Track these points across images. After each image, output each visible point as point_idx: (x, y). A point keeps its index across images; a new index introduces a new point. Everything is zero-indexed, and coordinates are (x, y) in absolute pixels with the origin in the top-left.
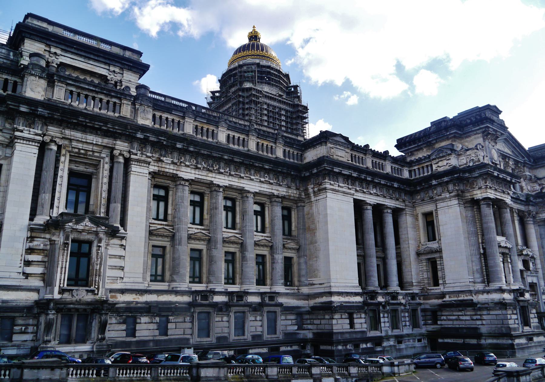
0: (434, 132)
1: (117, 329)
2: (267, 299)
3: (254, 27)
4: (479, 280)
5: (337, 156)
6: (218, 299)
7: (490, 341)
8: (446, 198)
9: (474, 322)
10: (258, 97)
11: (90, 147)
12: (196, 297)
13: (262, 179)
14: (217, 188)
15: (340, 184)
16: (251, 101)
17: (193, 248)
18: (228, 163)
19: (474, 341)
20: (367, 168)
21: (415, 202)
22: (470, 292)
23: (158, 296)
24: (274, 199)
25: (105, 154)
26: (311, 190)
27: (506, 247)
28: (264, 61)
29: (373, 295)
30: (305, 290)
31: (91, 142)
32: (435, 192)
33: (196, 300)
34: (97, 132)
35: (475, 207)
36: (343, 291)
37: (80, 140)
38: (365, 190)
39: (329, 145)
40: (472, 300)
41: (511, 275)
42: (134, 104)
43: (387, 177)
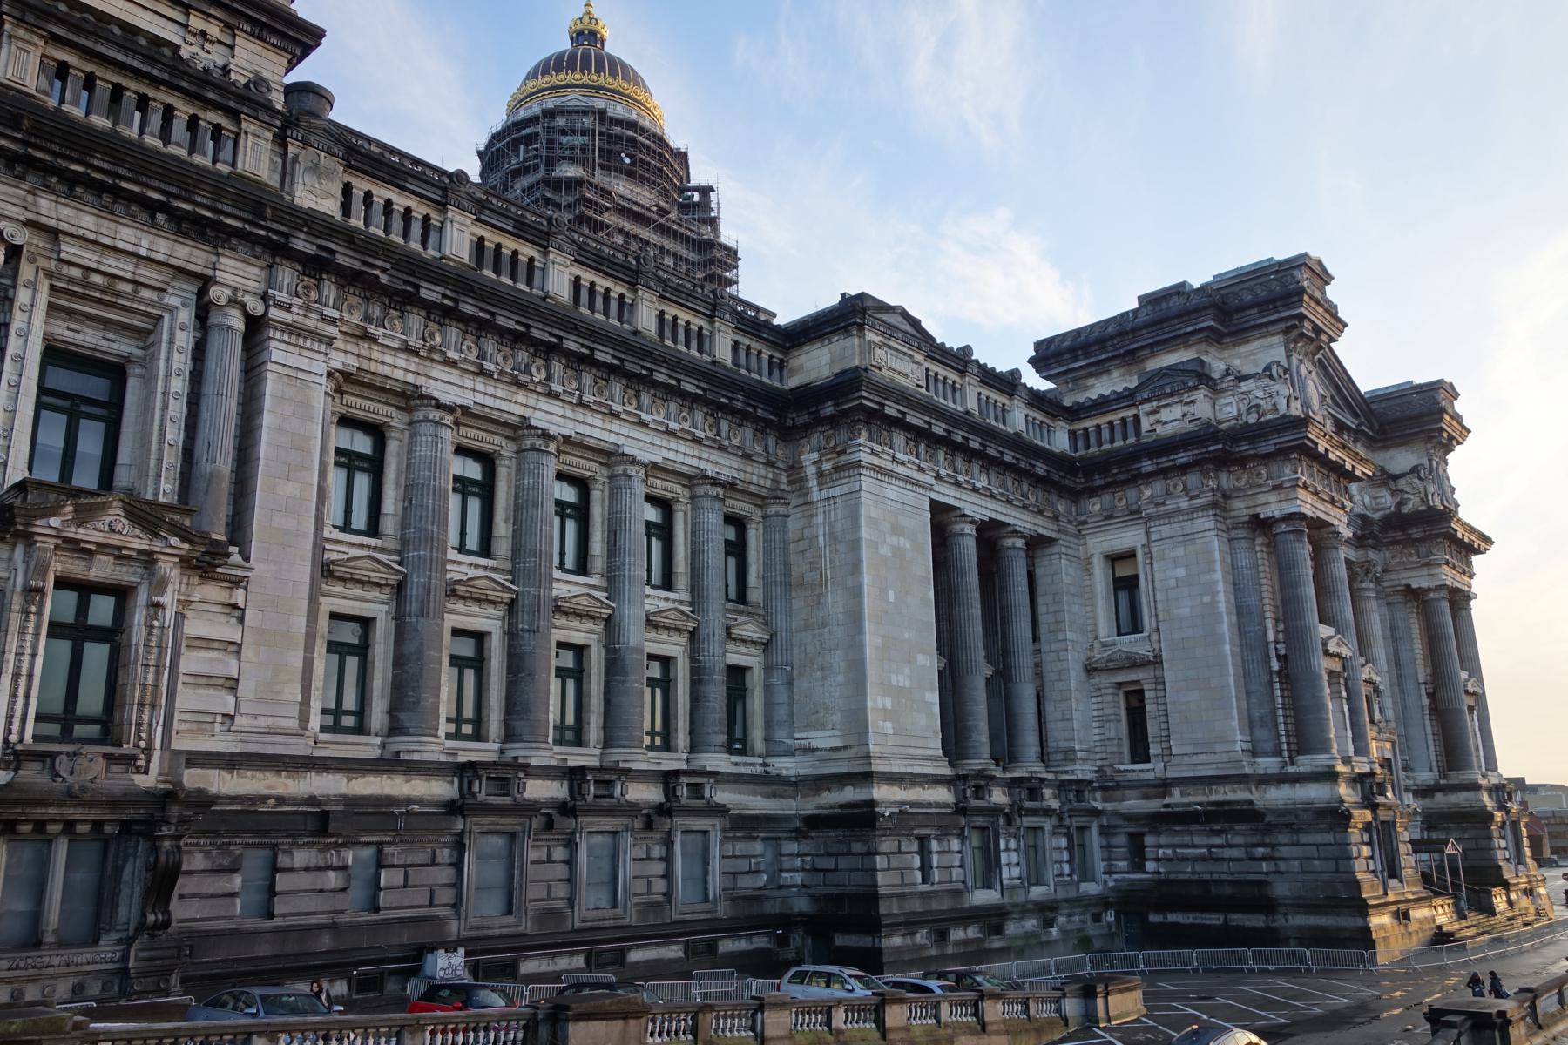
0: (1148, 325)
1: (211, 891)
2: (683, 792)
3: (588, 5)
4: (1268, 746)
5: (890, 369)
6: (539, 790)
7: (1299, 920)
8: (1178, 512)
9: (1254, 865)
10: (600, 209)
11: (123, 268)
12: (470, 784)
13: (674, 426)
14: (539, 443)
15: (900, 456)
17: (459, 626)
19: (1255, 921)
20: (968, 413)
21: (1085, 522)
22: (1243, 779)
23: (349, 780)
24: (701, 490)
26: (811, 470)
27: (1338, 656)
28: (619, 107)
29: (981, 783)
30: (787, 766)
31: (130, 248)
32: (1148, 493)
33: (473, 794)
34: (153, 217)
35: (1259, 540)
36: (903, 770)
37: (92, 236)
38: (961, 478)
39: (870, 336)
40: (1251, 802)
41: (1349, 734)
42: (281, 140)
43: (1015, 442)
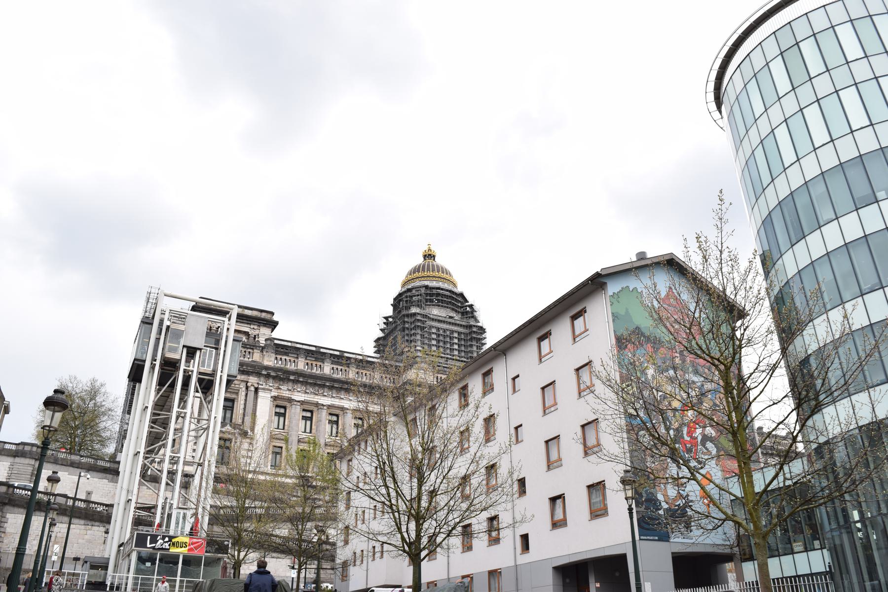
10: (424, 322)
16: (416, 327)
18: (331, 388)
25: (243, 386)
42: (262, 351)
